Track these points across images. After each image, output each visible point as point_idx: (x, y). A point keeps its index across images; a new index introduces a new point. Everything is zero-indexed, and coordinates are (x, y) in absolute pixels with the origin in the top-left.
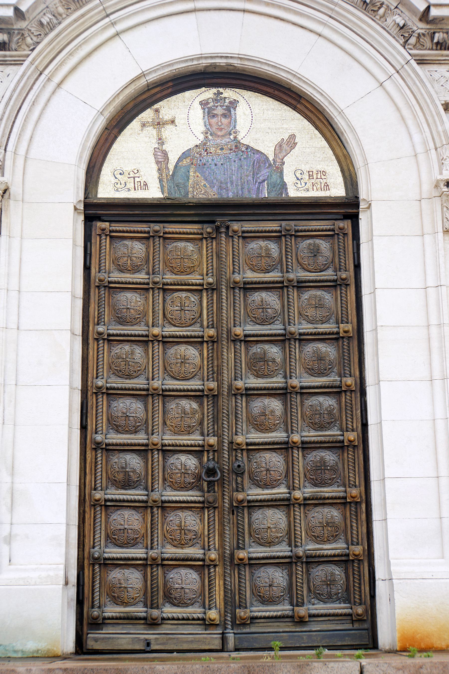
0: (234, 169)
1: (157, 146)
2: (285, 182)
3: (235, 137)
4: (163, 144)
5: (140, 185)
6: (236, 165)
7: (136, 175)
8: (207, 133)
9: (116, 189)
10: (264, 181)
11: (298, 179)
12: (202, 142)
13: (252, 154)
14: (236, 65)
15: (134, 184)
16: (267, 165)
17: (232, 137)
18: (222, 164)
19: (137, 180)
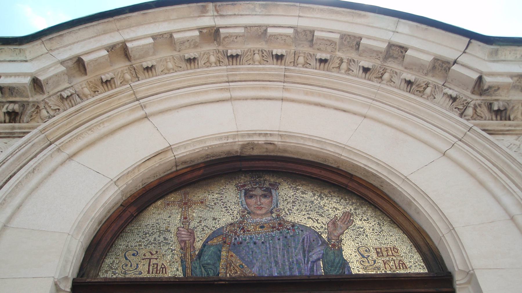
0: (278, 247)
5: (157, 268)
7: (153, 257)
8: (243, 212)
10: (319, 259)
13: (300, 232)
14: (276, 143)
16: (320, 242)
17: (274, 215)
18: (263, 243)
19: (154, 261)
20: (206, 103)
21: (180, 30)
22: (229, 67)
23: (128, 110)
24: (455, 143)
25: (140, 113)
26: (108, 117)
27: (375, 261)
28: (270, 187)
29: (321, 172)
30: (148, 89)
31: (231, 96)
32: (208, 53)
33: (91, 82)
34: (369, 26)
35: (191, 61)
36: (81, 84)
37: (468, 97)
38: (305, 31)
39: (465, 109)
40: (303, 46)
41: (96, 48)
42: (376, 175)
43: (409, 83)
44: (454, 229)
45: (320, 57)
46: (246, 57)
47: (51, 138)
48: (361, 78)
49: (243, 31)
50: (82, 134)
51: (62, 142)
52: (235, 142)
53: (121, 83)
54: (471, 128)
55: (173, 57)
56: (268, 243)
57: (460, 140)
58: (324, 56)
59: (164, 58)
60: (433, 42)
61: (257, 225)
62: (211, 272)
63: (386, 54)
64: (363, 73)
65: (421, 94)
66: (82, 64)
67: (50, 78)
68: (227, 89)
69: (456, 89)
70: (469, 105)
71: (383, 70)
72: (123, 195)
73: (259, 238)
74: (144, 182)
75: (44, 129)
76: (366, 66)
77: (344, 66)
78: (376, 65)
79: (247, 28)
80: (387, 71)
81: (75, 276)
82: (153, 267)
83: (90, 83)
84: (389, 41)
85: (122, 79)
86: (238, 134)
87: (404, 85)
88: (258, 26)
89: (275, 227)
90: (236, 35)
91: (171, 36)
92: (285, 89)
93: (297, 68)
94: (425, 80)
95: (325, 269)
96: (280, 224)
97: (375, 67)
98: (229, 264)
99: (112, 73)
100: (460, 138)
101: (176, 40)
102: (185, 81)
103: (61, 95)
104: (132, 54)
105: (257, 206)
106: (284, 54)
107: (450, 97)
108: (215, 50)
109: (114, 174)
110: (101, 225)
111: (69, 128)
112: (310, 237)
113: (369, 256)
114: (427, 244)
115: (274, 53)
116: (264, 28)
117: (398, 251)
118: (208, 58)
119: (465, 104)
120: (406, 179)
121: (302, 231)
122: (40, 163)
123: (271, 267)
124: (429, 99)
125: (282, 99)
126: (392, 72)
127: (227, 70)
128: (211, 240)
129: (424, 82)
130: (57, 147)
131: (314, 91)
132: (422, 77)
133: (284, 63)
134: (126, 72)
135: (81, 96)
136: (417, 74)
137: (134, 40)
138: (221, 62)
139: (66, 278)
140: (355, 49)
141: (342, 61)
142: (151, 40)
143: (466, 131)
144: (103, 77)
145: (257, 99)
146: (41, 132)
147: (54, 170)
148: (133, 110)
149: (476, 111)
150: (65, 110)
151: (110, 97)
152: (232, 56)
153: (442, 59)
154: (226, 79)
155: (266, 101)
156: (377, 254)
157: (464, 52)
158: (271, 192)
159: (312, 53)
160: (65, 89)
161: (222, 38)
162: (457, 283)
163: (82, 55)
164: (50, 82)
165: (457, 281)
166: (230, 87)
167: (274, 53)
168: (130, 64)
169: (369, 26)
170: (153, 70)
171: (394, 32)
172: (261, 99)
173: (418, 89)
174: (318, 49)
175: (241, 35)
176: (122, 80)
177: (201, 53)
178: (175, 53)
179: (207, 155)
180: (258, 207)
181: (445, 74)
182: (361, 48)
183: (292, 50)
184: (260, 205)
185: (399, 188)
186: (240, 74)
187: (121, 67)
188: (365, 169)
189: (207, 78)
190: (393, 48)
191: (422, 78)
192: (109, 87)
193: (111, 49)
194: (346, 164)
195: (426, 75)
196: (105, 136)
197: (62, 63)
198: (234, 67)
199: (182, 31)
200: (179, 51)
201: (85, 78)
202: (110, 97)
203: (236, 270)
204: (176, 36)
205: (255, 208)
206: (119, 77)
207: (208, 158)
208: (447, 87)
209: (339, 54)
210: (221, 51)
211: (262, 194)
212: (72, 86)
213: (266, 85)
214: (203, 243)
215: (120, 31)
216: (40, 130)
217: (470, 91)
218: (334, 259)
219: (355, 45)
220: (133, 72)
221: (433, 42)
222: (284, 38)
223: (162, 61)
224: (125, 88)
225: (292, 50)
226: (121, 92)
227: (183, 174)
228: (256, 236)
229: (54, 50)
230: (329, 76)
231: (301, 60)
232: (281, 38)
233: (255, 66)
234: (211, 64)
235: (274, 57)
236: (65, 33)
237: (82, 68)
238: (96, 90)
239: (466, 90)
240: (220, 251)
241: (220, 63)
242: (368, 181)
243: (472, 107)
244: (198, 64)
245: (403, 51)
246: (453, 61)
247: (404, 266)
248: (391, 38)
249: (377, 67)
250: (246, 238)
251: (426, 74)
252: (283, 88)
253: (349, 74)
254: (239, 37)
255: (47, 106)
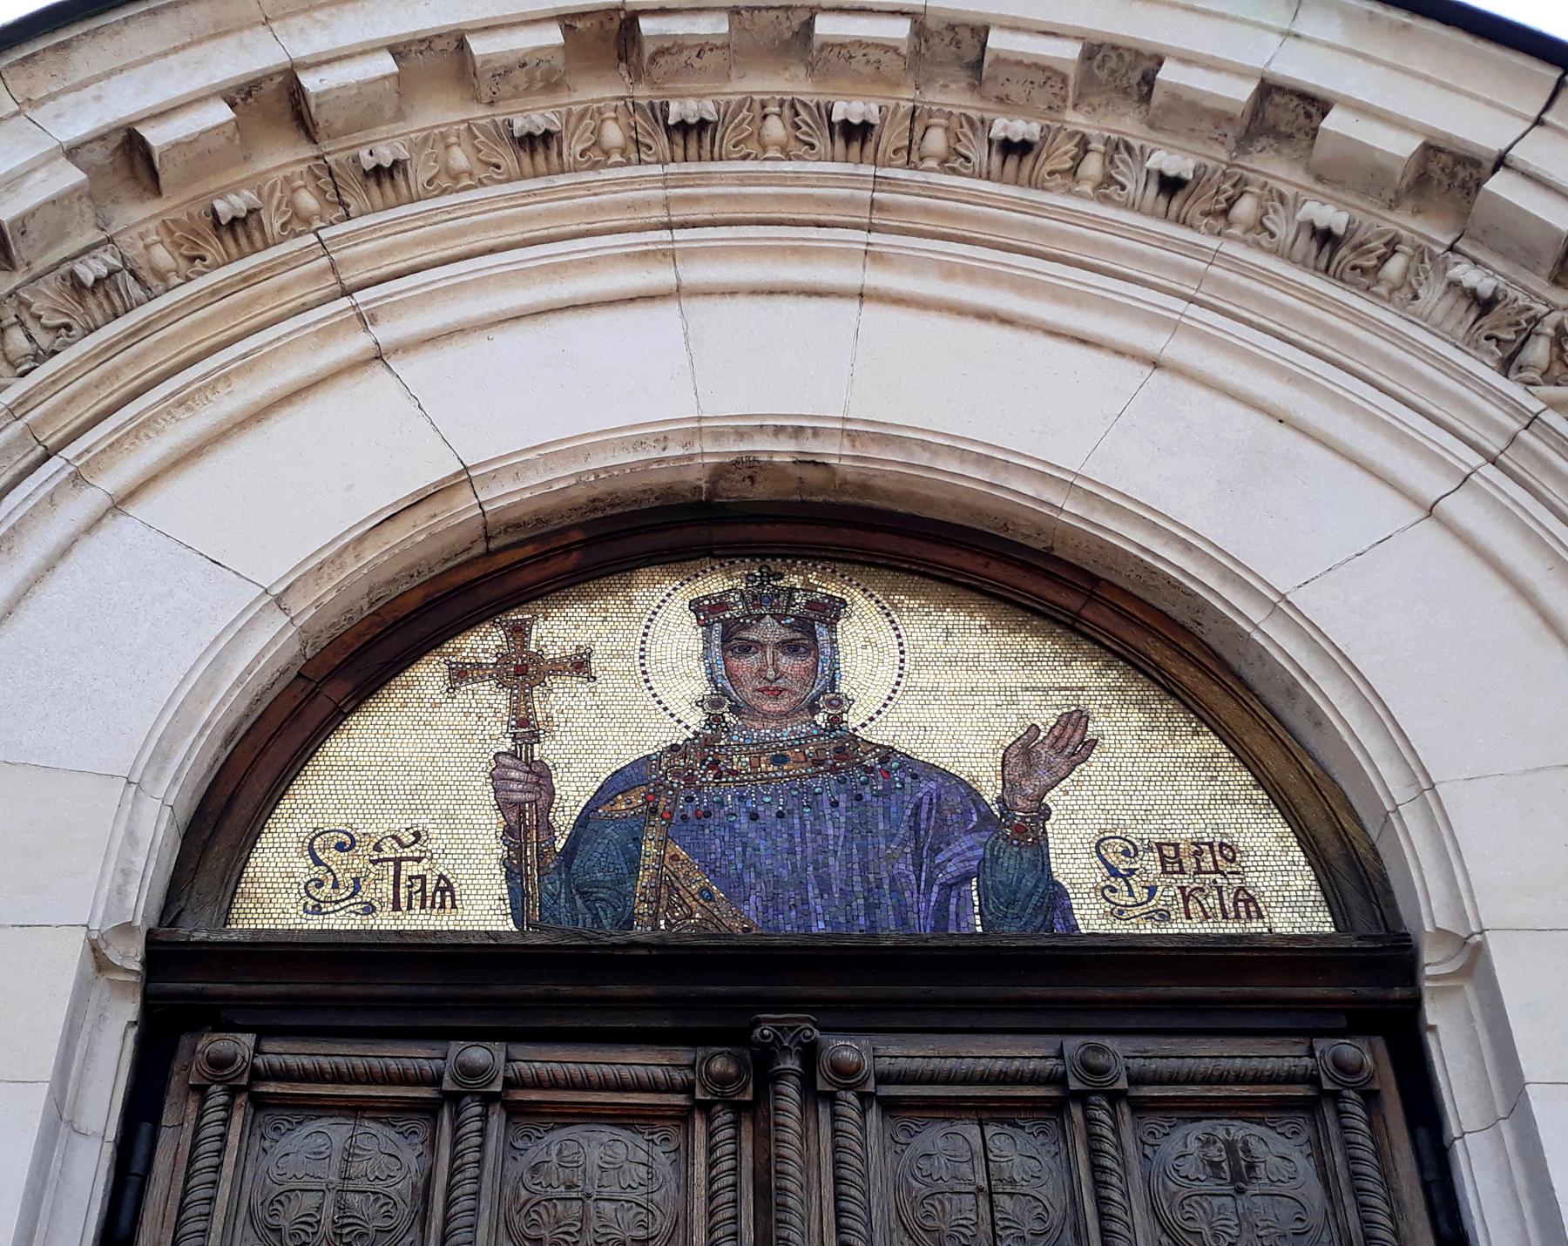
0: (831, 832)
1: (508, 745)
2: (1059, 884)
3: (835, 722)
4: (535, 737)
5: (423, 889)
6: (843, 819)
8: (716, 704)
9: (311, 902)
10: (966, 878)
11: (1114, 872)
12: (695, 733)
13: (908, 780)
15: (396, 885)
16: (975, 818)
17: (820, 719)
18: (780, 815)
20: (588, 305)
21: (493, 23)
22: (672, 168)
23: (312, 329)
24: (1474, 471)
25: (356, 344)
26: (245, 355)
27: (1152, 891)
28: (812, 615)
29: (987, 565)
30: (381, 253)
31: (678, 279)
32: (594, 113)
33: (175, 221)
34: (1193, 10)
35: (535, 143)
36: (142, 229)
37: (1539, 297)
38: (952, 27)
39: (1523, 343)
40: (945, 86)
41: (189, 94)
42: (1181, 583)
43: (1325, 238)
44: (1432, 787)
45: (1002, 135)
46: (735, 128)
47: (48, 434)
48: (1152, 214)
49: (725, 29)
50: (153, 419)
51: (87, 451)
52: (691, 457)
53: (284, 226)
54: (1536, 417)
55: (469, 129)
56: (796, 816)
57: (1494, 461)
58: (1020, 128)
59: (436, 131)
60: (1427, 79)
61: (762, 753)
62: (605, 911)
63: (1252, 121)
64: (1160, 197)
65: (1365, 281)
66: (141, 154)
67: (32, 213)
68: (664, 255)
69: (1497, 264)
70: (1538, 327)
71: (1234, 186)
72: (304, 644)
73: (767, 799)
74: (374, 596)
75: (23, 401)
76: (1171, 172)
77: (1093, 166)
78: (1211, 164)
79: (738, 13)
80: (1248, 188)
81: (153, 923)
82: (409, 887)
83: (172, 227)
84: (1263, 72)
85: (285, 213)
86: (700, 428)
87: (1306, 245)
88: (780, 8)
89: (822, 762)
90: (697, 45)
91: (462, 45)
92: (872, 256)
93: (918, 176)
94: (1386, 226)
95: (986, 913)
96: (840, 752)
97: (1204, 173)
98: (666, 886)
99: (251, 190)
100: (1495, 451)
101: (478, 65)
102: (513, 220)
103: (73, 274)
104: (320, 116)
105: (765, 684)
106: (874, 119)
107: (1472, 295)
108: (622, 98)
109: (274, 570)
110: (230, 747)
111: (107, 397)
112: (939, 797)
113: (1132, 872)
114: (1341, 835)
115: (837, 117)
116: (806, 16)
117: (1234, 857)
118: (598, 131)
119: (1525, 325)
120: (1281, 605)
121: (915, 776)
122: (13, 527)
123: (805, 902)
124: (1397, 300)
125: (861, 295)
126: (1266, 192)
127: (664, 182)
128: (608, 802)
129: (1381, 235)
130: (72, 469)
131: (976, 264)
132: (1375, 215)
133: (872, 151)
134: (300, 183)
135: (143, 274)
136: (1356, 202)
137: (328, 62)
138: (643, 149)
139: (126, 928)
140: (1136, 98)
141: (1084, 146)
142: (386, 64)
143: (1515, 426)
144: (220, 206)
145: (771, 293)
146: (11, 411)
147: (64, 551)
148: (329, 332)
149: (1563, 350)
150: (91, 332)
151: (247, 280)
152: (683, 127)
153: (1454, 149)
154: (659, 215)
155: (802, 298)
156: (1163, 865)
157: (1539, 122)
158: (812, 634)
159: (974, 115)
160: (87, 250)
161: (647, 56)
162: (1428, 971)
163: (141, 121)
164: (32, 226)
165: (1428, 965)
166: (677, 245)
167: (837, 117)
168: (316, 153)
169: (1193, 10)
170: (399, 178)
171: (1288, 34)
172: (784, 292)
173: (1358, 262)
174: (1000, 100)
175: (719, 42)
176: (289, 214)
177: (569, 113)
178: (479, 112)
179: (594, 500)
180: (767, 689)
181: (1465, 203)
182: (1158, 96)
183: (902, 103)
184: (776, 679)
185: (1256, 636)
186: (711, 197)
187: (286, 165)
188: (1142, 561)
189: (592, 209)
190: (1277, 98)
191: (1375, 220)
192: (243, 241)
193: (242, 95)
194: (1076, 542)
195: (1390, 208)
196: (235, 426)
197: (72, 152)
198: (693, 167)
199: (501, 26)
200: (491, 103)
201: (154, 207)
202: (247, 280)
203: (690, 908)
204: (479, 46)
205: (758, 690)
206: (275, 202)
207: (596, 509)
208: (1465, 255)
209: (1076, 120)
210: (644, 103)
211: (784, 642)
212: (110, 240)
213: (804, 239)
214: (582, 812)
215: (275, 25)
216: (7, 407)
217: (1545, 272)
218: (1020, 880)
219: (1139, 84)
220: (325, 183)
221: (1427, 79)
222: (874, 54)
223: (431, 142)
224: (301, 249)
225: (902, 103)
226: (284, 263)
227: (512, 569)
228: (757, 790)
229: (42, 102)
230: (1035, 208)
231: (936, 141)
232: (864, 55)
233: (768, 166)
234: (607, 153)
235: (837, 128)
236: (77, 36)
237: (141, 169)
238: (195, 253)
239: (1534, 270)
240: (637, 841)
241: (639, 152)
242: (1153, 602)
243: (1546, 335)
244: (560, 154)
245: (1313, 110)
246: (1494, 157)
247: (1252, 909)
248: (1269, 63)
249: (1215, 172)
250: (723, 797)
251: (1392, 205)
252: (866, 252)
253: (1106, 199)
254: (711, 50)
255: (25, 316)
